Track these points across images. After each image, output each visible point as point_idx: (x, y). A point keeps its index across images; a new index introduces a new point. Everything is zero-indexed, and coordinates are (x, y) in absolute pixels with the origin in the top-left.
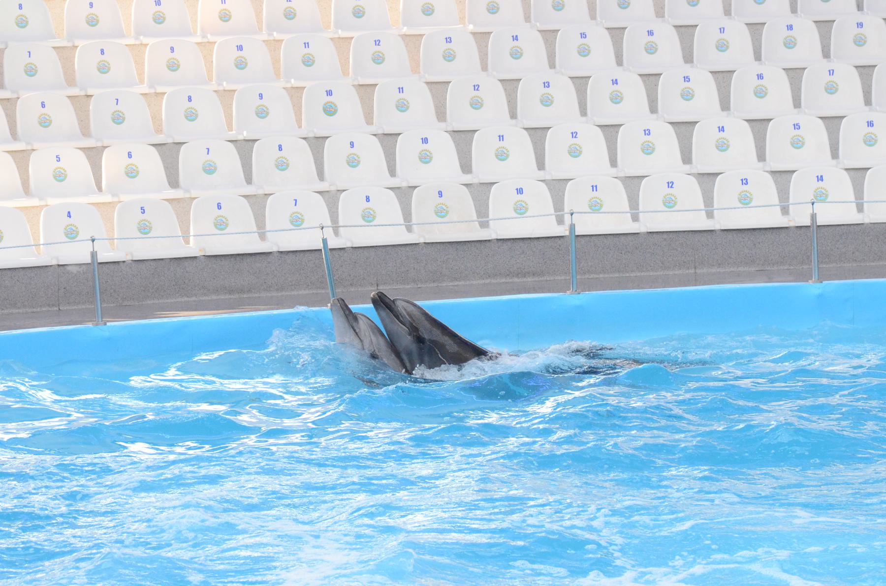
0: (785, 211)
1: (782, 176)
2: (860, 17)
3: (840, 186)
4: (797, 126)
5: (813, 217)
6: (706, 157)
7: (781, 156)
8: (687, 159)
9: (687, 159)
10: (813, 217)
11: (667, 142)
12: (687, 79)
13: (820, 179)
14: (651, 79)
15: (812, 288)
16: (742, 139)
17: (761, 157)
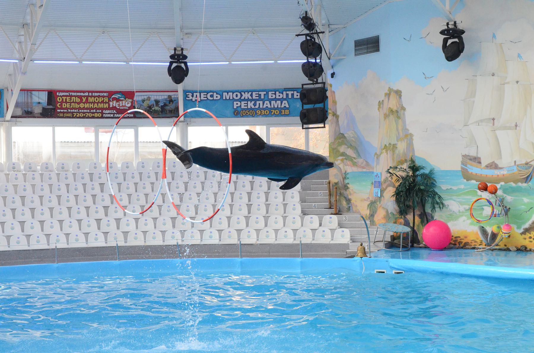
0: (49, 245)
1: (48, 236)
2: (68, 195)
3: (63, 239)
4: (52, 223)
5: (56, 247)
6: (28, 231)
7: (47, 230)
8: (23, 231)
9: (23, 231)
10: (56, 247)
11: (18, 227)
12: (23, 210)
13: (58, 236)
14: (13, 210)
15: (55, 265)
16: (38, 226)
17: (42, 230)
